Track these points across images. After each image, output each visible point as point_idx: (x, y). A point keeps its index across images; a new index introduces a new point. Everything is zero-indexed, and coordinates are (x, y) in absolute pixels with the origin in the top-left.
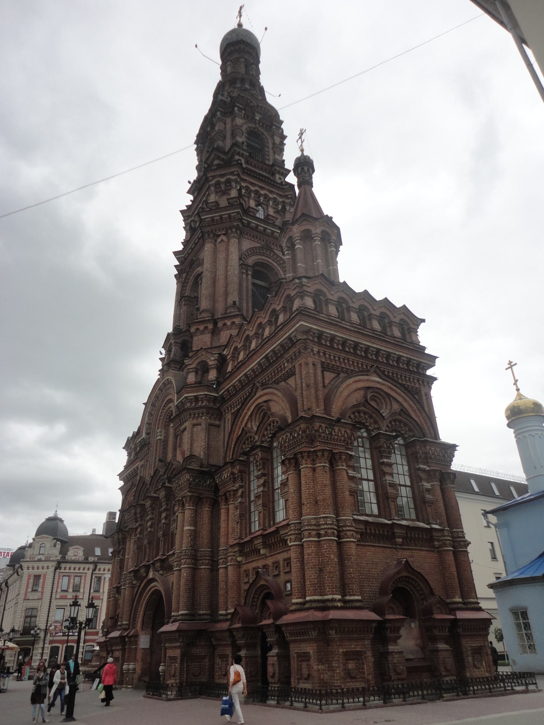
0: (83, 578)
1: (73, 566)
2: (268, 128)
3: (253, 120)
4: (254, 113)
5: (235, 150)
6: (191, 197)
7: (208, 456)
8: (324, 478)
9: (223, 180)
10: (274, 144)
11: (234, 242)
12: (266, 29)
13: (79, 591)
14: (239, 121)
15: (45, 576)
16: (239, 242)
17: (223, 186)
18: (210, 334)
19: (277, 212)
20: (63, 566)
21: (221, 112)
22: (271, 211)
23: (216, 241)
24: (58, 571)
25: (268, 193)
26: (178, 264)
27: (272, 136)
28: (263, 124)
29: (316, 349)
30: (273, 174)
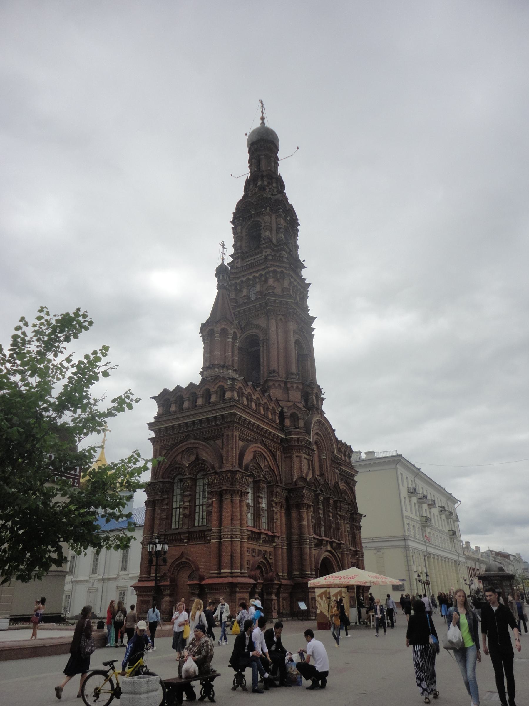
9: (279, 270)
12: (298, 148)
14: (282, 222)
17: (279, 276)
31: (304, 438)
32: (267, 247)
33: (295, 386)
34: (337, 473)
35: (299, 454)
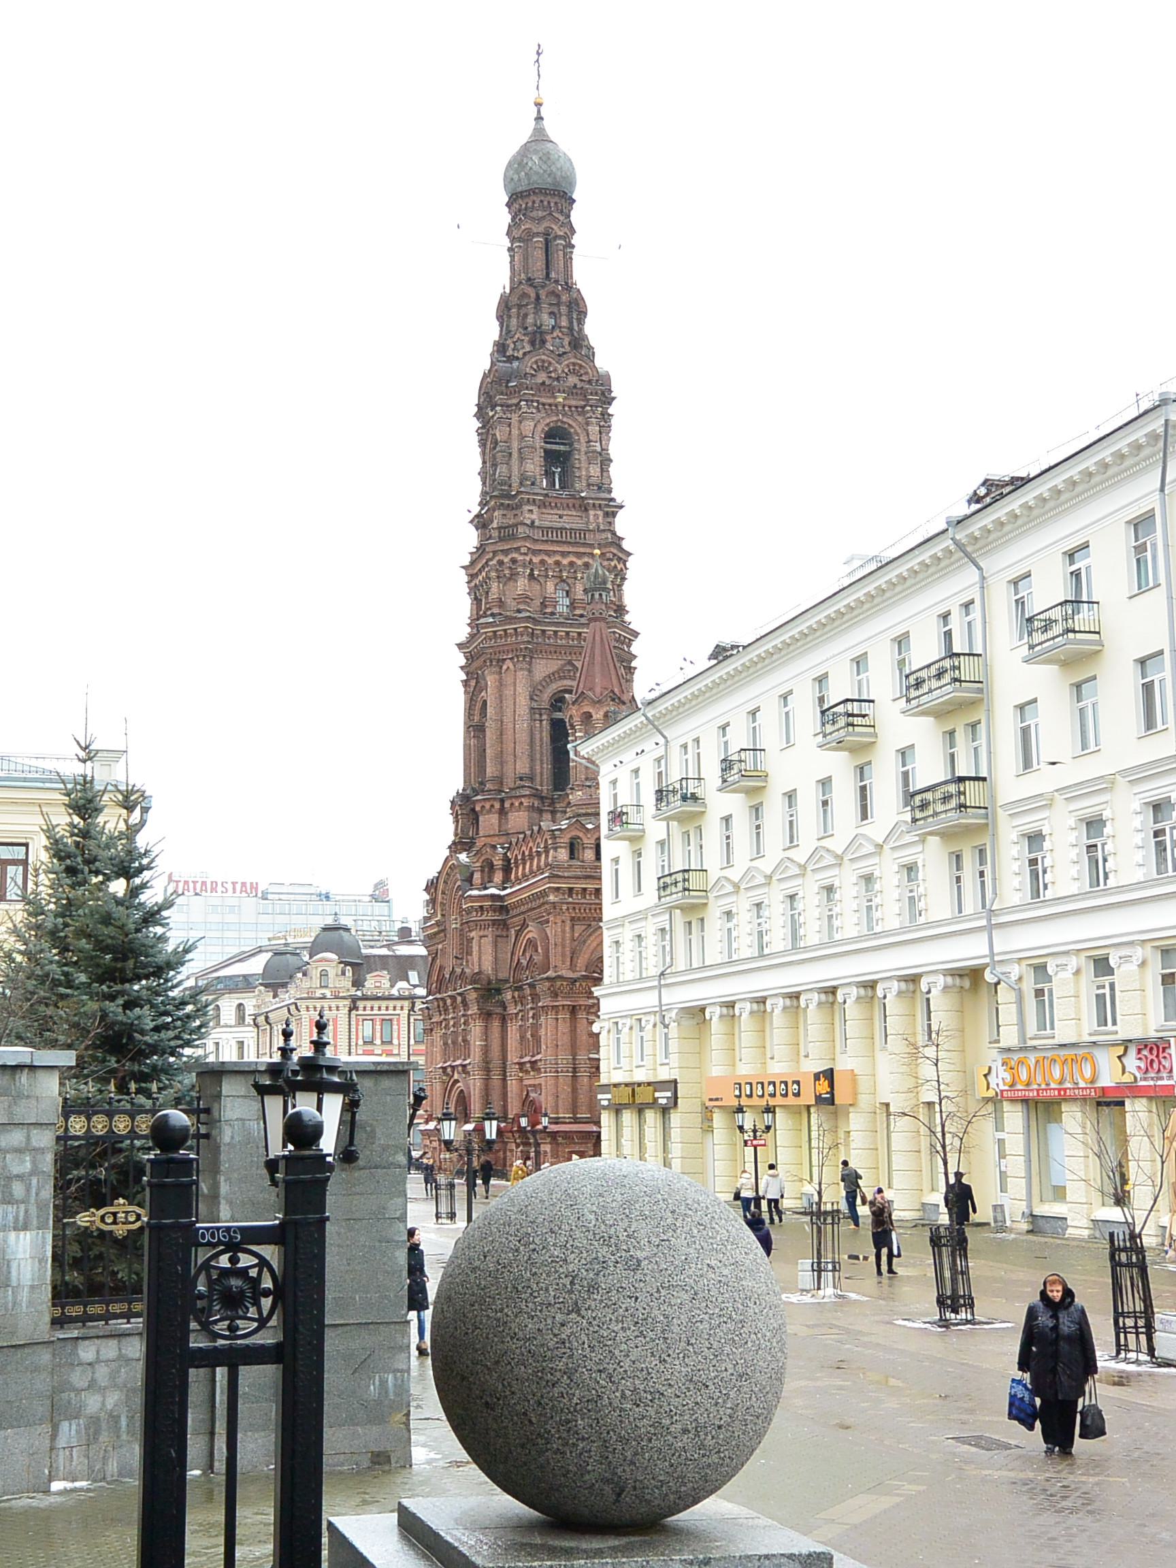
0: (395, 1022)
1: (376, 1004)
7: (496, 970)
8: (564, 1027)
13: (391, 1043)
15: (335, 1020)
16: (530, 671)
18: (496, 816)
20: (361, 1004)
24: (354, 1012)
25: (574, 559)
26: (463, 662)
29: (565, 907)
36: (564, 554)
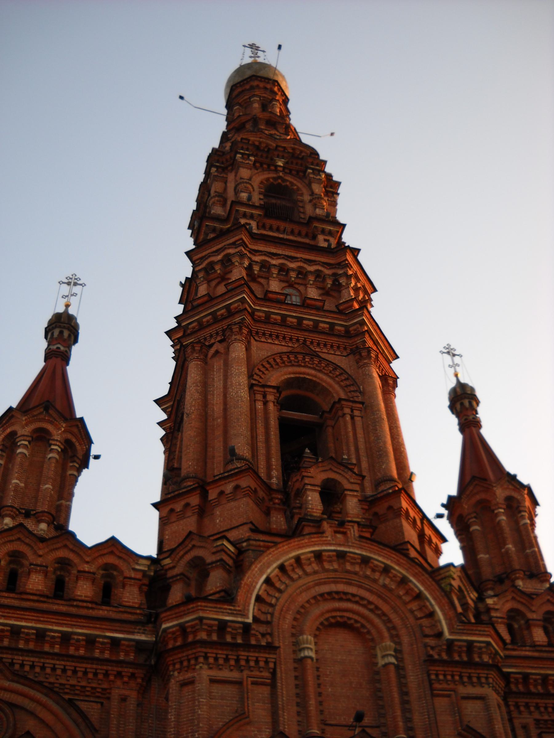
2: (301, 174)
3: (271, 166)
4: (272, 159)
5: (237, 211)
6: (182, 306)
9: (219, 257)
10: (312, 194)
11: (238, 350)
14: (245, 173)
17: (218, 267)
19: (326, 293)
21: (217, 167)
22: (313, 293)
23: (206, 356)
27: (309, 185)
28: (291, 170)
30: (314, 237)
31: (201, 619)
32: (207, 235)
33: (229, 488)
34: (481, 698)
35: (190, 675)
36: (292, 259)
